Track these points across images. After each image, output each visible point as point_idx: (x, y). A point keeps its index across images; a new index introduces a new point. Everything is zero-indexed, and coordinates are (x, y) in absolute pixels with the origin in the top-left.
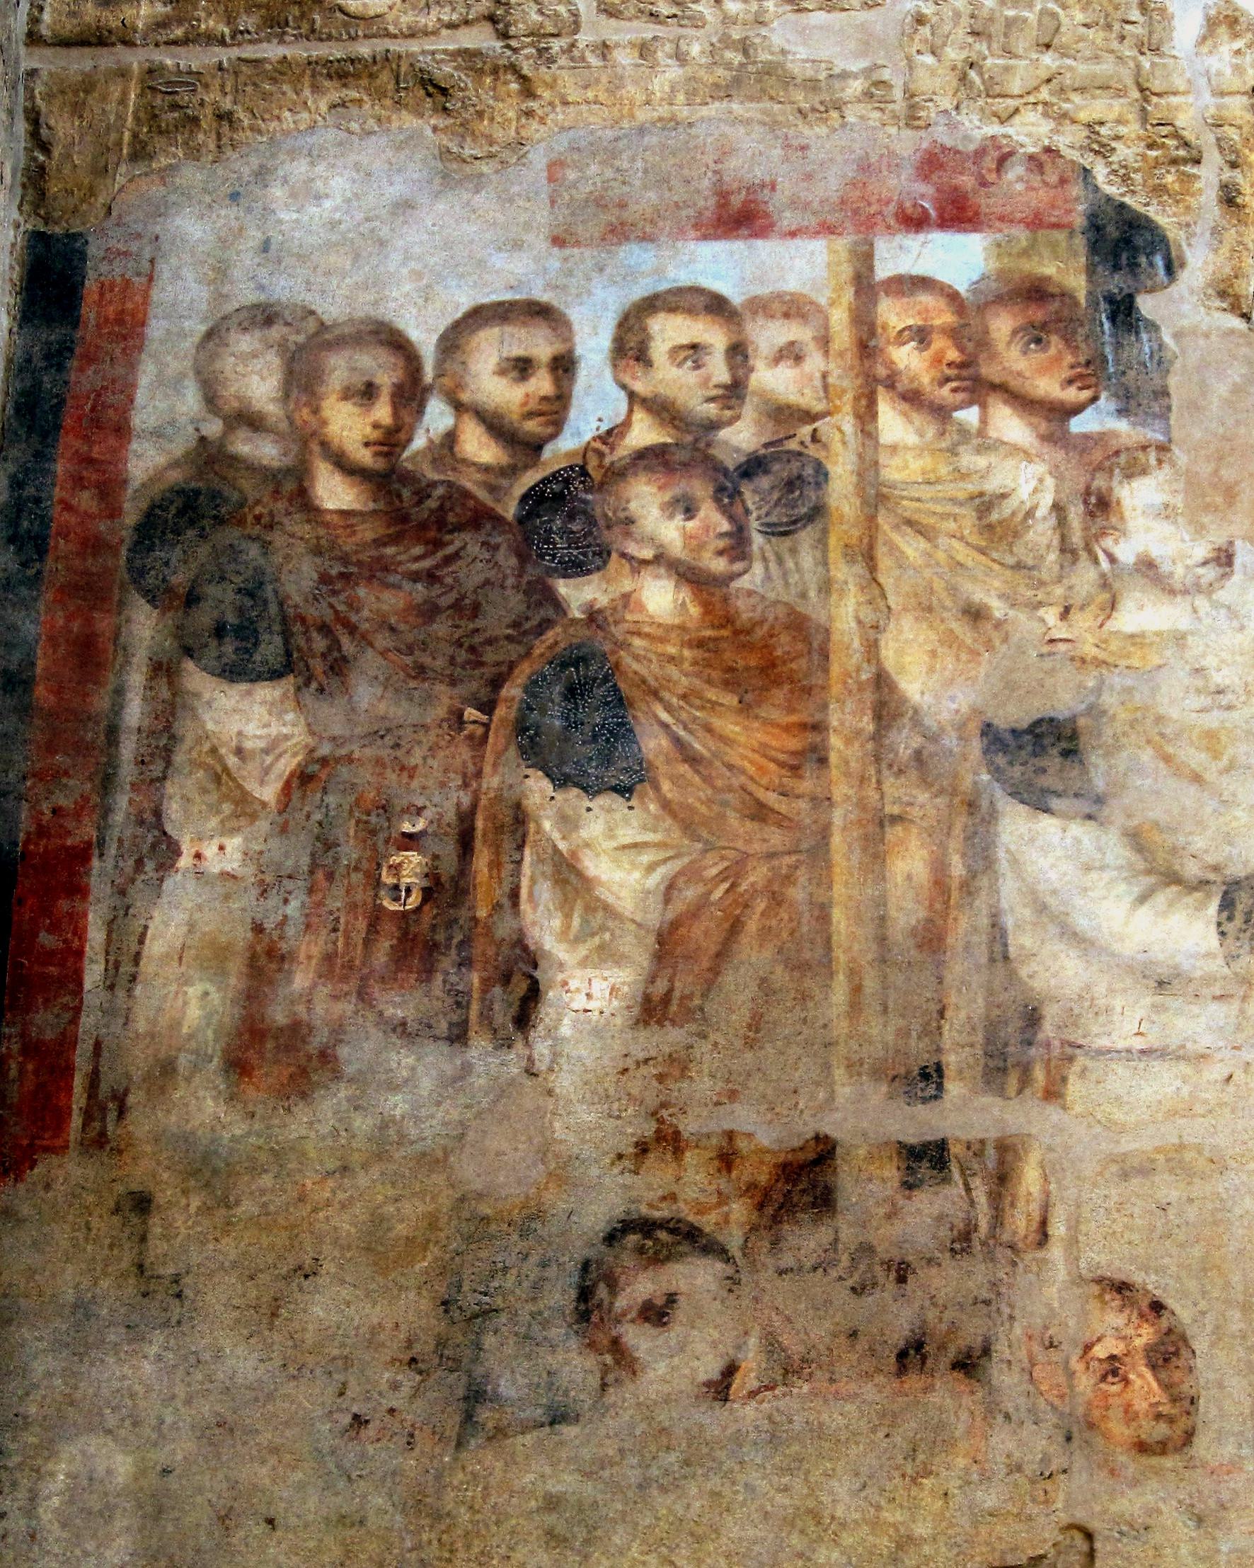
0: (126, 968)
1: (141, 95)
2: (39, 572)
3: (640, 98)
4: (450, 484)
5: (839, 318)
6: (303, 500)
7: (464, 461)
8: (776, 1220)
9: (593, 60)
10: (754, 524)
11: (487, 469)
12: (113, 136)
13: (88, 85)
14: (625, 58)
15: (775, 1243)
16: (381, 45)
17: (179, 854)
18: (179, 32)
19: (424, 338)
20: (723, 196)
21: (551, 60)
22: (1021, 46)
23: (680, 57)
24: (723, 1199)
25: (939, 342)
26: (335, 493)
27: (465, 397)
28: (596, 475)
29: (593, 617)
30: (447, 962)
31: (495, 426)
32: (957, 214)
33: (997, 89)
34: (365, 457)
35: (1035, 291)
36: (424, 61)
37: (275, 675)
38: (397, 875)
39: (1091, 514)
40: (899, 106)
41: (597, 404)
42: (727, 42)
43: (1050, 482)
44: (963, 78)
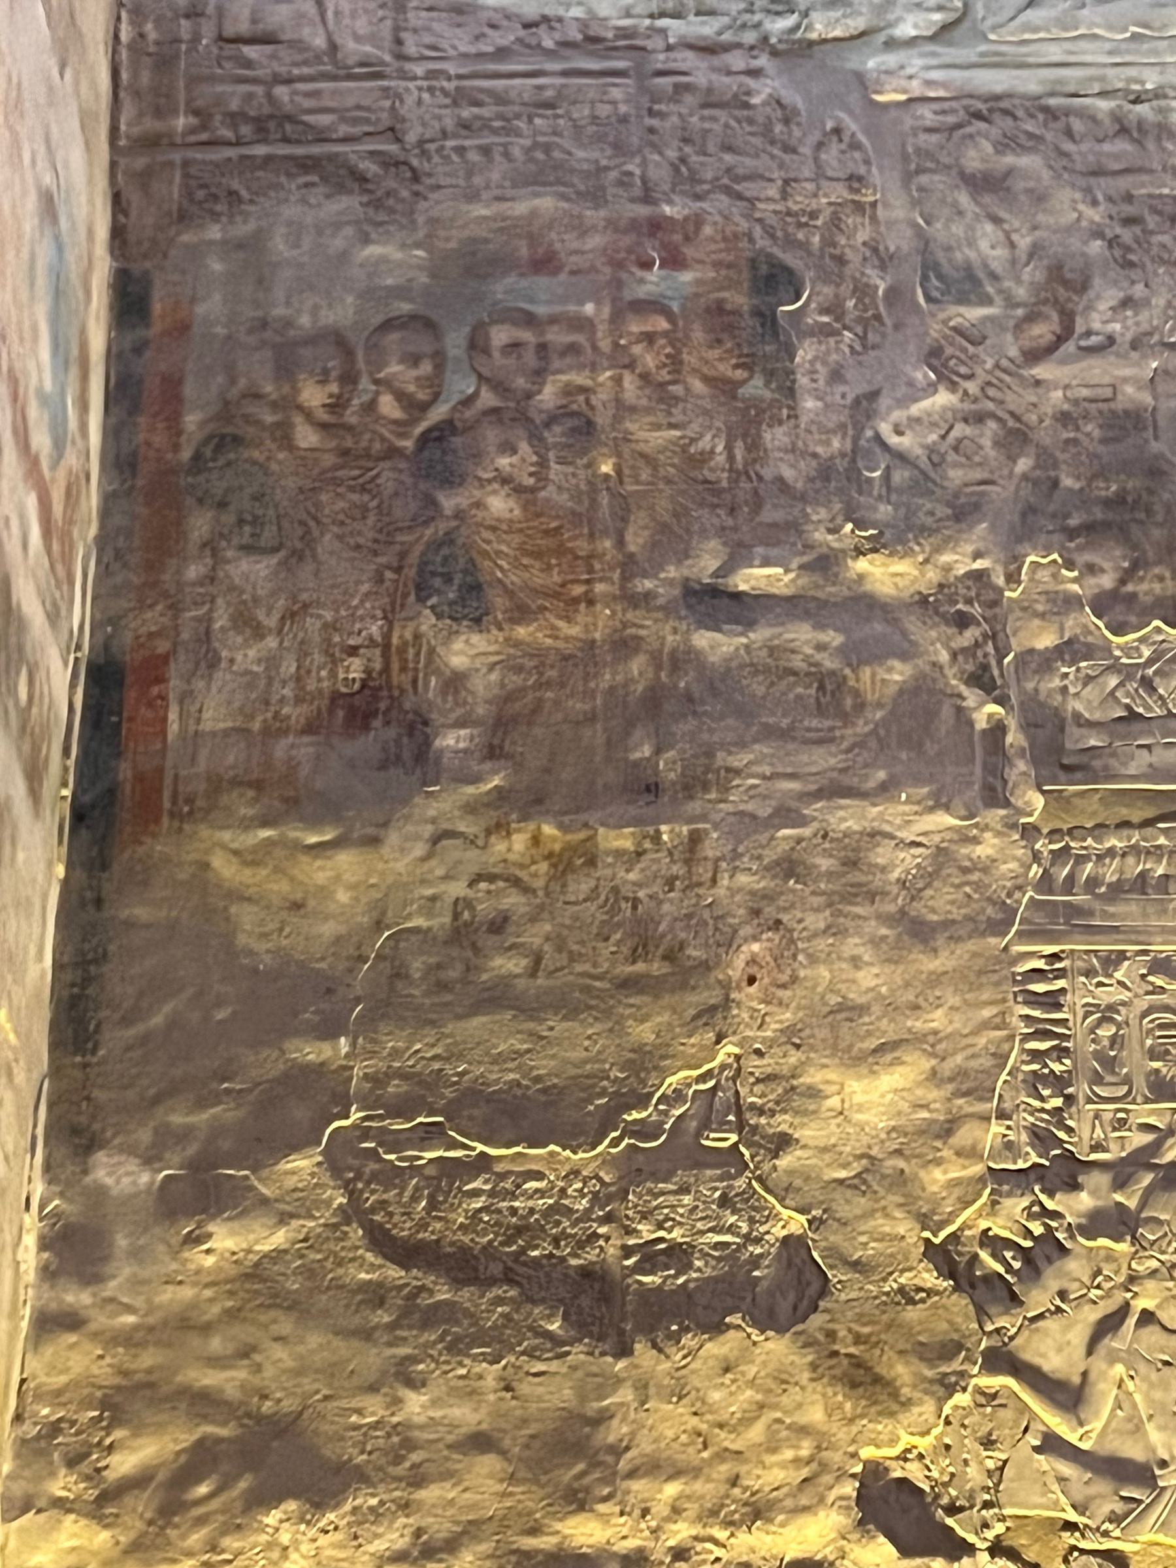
2: (132, 487)
8: (564, 872)
9: (455, 158)
10: (551, 455)
11: (396, 422)
15: (564, 886)
17: (220, 660)
18: (204, 137)
21: (429, 160)
22: (711, 148)
23: (506, 155)
24: (534, 862)
26: (306, 437)
27: (382, 375)
28: (459, 424)
29: (459, 515)
30: (377, 723)
31: (401, 397)
32: (674, 261)
34: (325, 417)
35: (719, 309)
37: (275, 550)
40: (637, 191)
42: (536, 145)
44: (677, 170)
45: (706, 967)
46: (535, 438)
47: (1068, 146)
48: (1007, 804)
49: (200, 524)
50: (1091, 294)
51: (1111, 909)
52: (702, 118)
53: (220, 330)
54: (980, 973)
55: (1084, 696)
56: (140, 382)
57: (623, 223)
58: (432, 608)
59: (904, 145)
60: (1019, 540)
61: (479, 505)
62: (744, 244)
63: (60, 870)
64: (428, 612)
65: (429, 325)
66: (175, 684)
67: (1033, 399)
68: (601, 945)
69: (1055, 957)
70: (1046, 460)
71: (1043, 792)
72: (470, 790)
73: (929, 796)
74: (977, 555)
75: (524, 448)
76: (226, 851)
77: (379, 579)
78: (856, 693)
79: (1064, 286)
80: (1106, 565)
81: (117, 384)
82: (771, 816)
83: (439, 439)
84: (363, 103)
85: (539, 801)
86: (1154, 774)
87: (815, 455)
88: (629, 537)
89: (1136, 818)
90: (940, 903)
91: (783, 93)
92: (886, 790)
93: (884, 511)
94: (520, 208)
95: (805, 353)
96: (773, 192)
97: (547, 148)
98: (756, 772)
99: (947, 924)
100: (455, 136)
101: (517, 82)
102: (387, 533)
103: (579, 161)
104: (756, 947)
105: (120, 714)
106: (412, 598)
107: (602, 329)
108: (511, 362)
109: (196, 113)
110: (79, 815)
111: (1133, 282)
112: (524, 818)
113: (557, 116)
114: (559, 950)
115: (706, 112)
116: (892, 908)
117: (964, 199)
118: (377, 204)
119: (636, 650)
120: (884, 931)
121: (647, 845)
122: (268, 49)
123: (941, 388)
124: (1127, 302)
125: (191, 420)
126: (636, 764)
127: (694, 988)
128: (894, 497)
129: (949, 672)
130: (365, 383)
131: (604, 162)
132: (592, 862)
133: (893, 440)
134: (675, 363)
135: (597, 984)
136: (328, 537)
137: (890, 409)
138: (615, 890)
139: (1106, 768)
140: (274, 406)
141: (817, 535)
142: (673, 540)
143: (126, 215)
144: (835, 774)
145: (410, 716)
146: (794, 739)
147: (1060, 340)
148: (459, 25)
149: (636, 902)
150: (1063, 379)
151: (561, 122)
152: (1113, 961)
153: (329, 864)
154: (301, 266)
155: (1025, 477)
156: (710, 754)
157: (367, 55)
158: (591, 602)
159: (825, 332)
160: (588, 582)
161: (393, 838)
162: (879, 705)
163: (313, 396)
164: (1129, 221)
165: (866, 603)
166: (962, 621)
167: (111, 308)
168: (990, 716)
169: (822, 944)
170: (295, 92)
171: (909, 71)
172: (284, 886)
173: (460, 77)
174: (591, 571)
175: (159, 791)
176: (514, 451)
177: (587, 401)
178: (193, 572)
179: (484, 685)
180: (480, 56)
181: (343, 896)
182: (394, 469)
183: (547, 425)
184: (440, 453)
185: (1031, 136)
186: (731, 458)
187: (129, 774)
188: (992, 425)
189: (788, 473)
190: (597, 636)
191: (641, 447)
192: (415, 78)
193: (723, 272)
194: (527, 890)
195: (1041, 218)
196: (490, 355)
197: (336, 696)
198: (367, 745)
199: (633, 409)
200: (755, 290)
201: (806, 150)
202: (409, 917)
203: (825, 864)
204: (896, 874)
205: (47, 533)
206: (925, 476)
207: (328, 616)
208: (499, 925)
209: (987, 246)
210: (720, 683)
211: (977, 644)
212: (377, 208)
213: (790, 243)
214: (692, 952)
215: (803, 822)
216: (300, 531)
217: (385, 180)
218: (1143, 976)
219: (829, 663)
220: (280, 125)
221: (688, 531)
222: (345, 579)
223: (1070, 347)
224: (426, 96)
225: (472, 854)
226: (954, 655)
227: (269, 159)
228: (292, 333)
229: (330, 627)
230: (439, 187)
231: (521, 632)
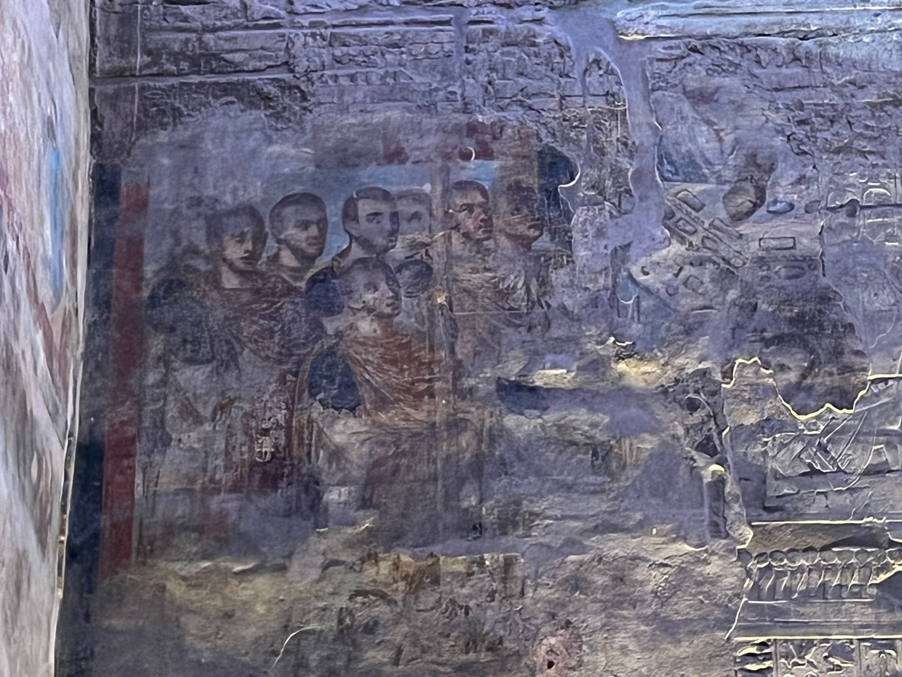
0: (152, 489)
1: (140, 99)
2: (108, 318)
3: (350, 101)
4: (277, 276)
5: (436, 202)
6: (217, 284)
7: (282, 266)
9: (330, 82)
10: (402, 292)
11: (293, 269)
12: (129, 119)
13: (116, 95)
15: (417, 598)
16: (241, 77)
17: (171, 439)
18: (155, 70)
19: (265, 212)
20: (387, 147)
21: (313, 84)
22: (510, 73)
23: (367, 81)
24: (396, 582)
25: (477, 210)
26: (230, 281)
27: (282, 237)
28: (337, 272)
29: (339, 335)
30: (283, 484)
32: (485, 153)
33: (501, 95)
34: (240, 265)
35: (517, 188)
37: (208, 361)
38: (261, 447)
39: (540, 286)
40: (459, 105)
41: (338, 242)
43: (523, 272)
45: (518, 655)
46: (391, 280)
47: (757, 71)
48: (727, 536)
49: (156, 345)
50: (777, 173)
51: (802, 610)
52: (502, 54)
53: (167, 206)
54: (711, 657)
55: (781, 459)
56: (113, 244)
57: (449, 128)
58: (320, 401)
59: (644, 71)
60: (731, 347)
61: (351, 327)
62: (534, 141)
63: (60, 593)
64: (317, 404)
66: (140, 459)
67: (738, 248)
68: (443, 640)
69: (764, 644)
70: (748, 290)
71: (752, 527)
72: (350, 530)
73: (672, 530)
74: (702, 359)
75: (383, 286)
76: (177, 575)
77: (282, 380)
78: (620, 457)
79: (757, 170)
80: (791, 365)
81: (96, 246)
82: (562, 546)
83: (322, 281)
84: (267, 46)
85: (398, 538)
86: (830, 513)
87: (586, 289)
88: (457, 349)
89: (819, 543)
90: (682, 607)
91: (559, 35)
92: (642, 527)
93: (636, 328)
94: (378, 118)
95: (579, 216)
96: (553, 104)
97: (395, 76)
98: (553, 513)
99: (687, 622)
100: (332, 67)
101: (373, 29)
102: (288, 350)
103: (419, 84)
104: (553, 641)
105: (101, 481)
106: (306, 394)
107: (436, 202)
108: (373, 225)
109: (149, 53)
110: (73, 554)
111: (805, 166)
112: (387, 551)
113: (402, 53)
114: (414, 644)
115: (506, 49)
116: (649, 611)
117: (686, 107)
118: (277, 116)
119: (465, 429)
120: (643, 628)
121: (475, 569)
123: (674, 241)
124: (801, 180)
125: (149, 270)
126: (466, 510)
127: (510, 671)
128: (642, 318)
129: (685, 442)
130: (271, 243)
131: (435, 85)
132: (436, 581)
133: (641, 278)
134: (487, 224)
135: (441, 669)
136: (246, 352)
137: (639, 256)
138: (453, 601)
139: (796, 509)
140: (207, 259)
141: (589, 346)
142: (489, 347)
143: (101, 126)
144: (606, 517)
145: (306, 478)
146: (576, 491)
147: (756, 206)
149: (467, 610)
151: (404, 56)
152: (803, 648)
153: (250, 586)
154: (224, 161)
155: (734, 303)
156: (518, 503)
158: (432, 396)
159: (591, 203)
160: (430, 381)
161: (295, 566)
162: (637, 466)
163: (235, 252)
164: (801, 123)
165: (625, 393)
166: (693, 406)
167: (92, 191)
168: (714, 472)
169: (600, 637)
170: (219, 38)
171: (646, 19)
172: (218, 602)
173: (334, 26)
174: (432, 373)
175: (130, 535)
176: (376, 289)
177: (427, 254)
178: (152, 378)
179: (359, 454)
181: (260, 609)
182: (293, 303)
183: (399, 270)
184: (325, 291)
185: (731, 63)
186: (528, 291)
187: (108, 524)
188: (710, 266)
189: (568, 303)
190: (437, 419)
191: (465, 285)
192: (302, 27)
193: (520, 161)
194: (391, 602)
195: (741, 121)
196: (358, 222)
197: (253, 465)
198: (276, 499)
199: (459, 258)
200: (542, 175)
201: (576, 74)
202: (308, 622)
203: (600, 580)
204: (649, 588)
205: (49, 359)
206: (664, 305)
207: (247, 407)
208: (371, 628)
209: (703, 141)
210: (522, 453)
211: (703, 422)
213: (566, 140)
214: (506, 644)
215: (583, 550)
216: (225, 348)
217: (280, 97)
218: (826, 657)
219: (600, 436)
220: (208, 62)
221: (499, 343)
222: (258, 382)
223: (762, 211)
224: (310, 40)
225: (351, 576)
226: (687, 431)
227: (201, 85)
228: (218, 207)
229: (250, 415)
230: (320, 104)
231: (383, 417)
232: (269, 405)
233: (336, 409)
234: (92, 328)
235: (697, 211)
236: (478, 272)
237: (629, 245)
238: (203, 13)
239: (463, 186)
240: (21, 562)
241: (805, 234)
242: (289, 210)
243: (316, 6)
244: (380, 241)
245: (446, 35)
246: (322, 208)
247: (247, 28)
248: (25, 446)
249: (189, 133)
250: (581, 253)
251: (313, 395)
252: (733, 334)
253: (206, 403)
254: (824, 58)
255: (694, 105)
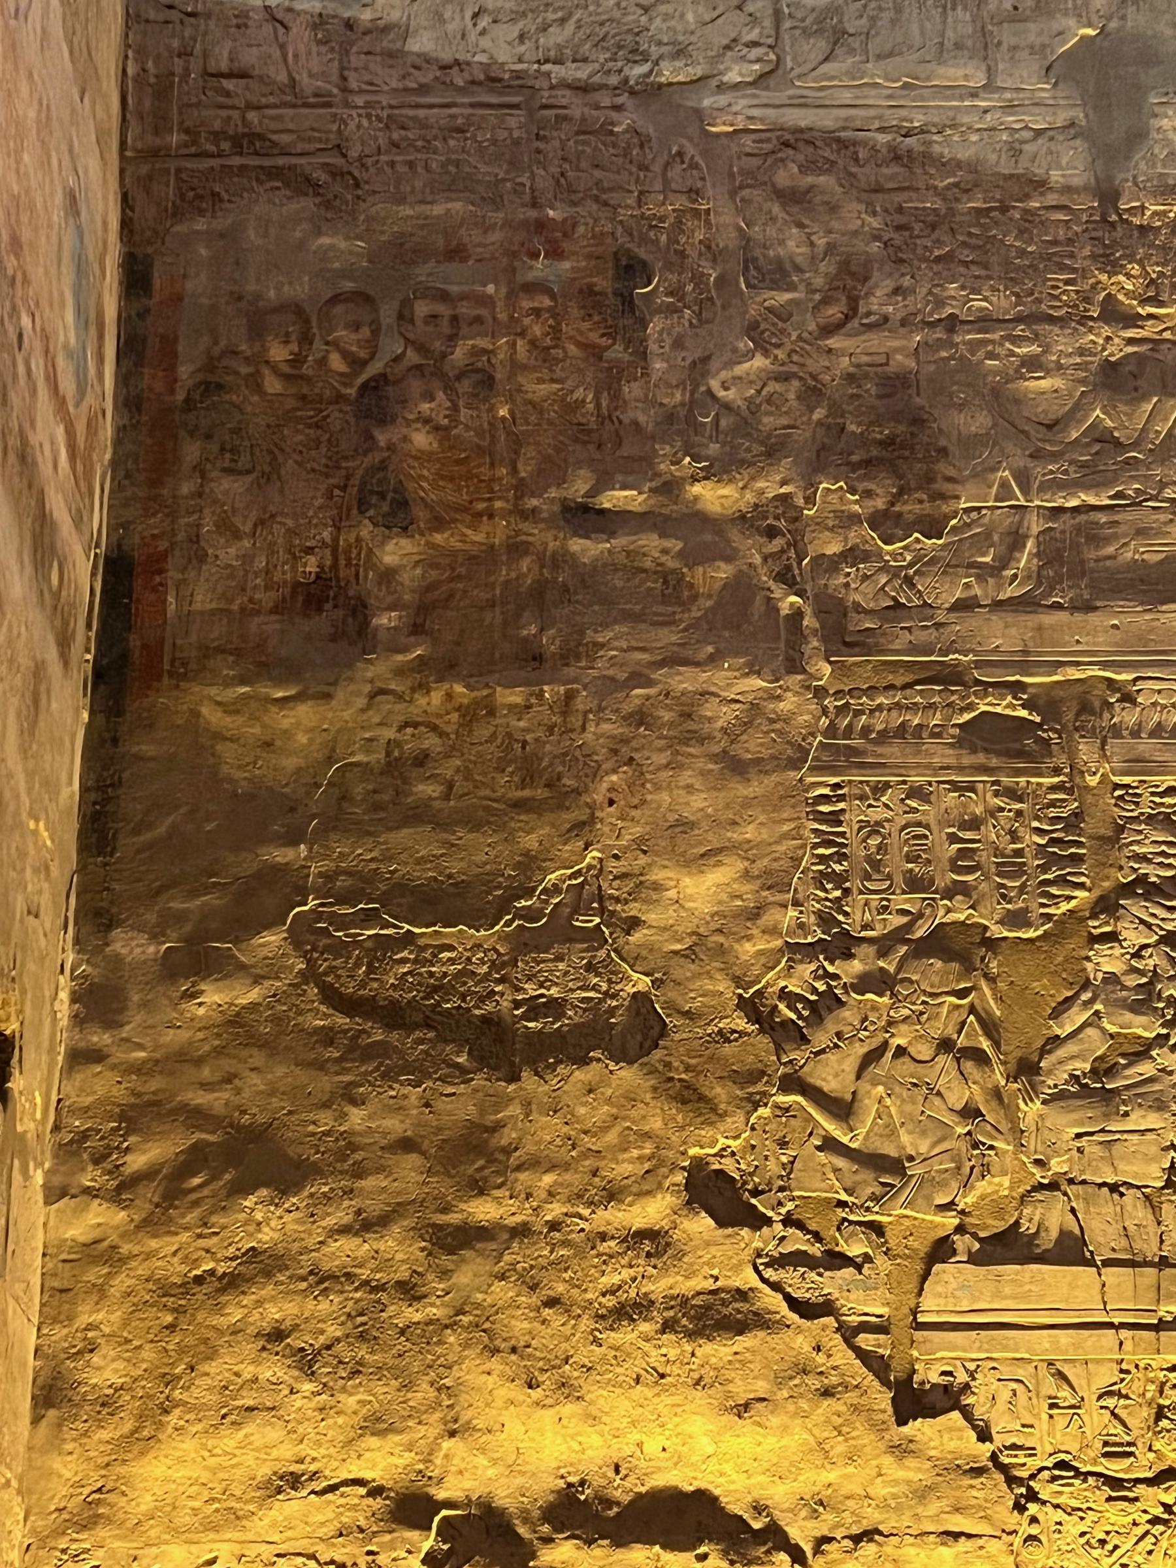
0: (186, 608)
3: (408, 189)
6: (258, 388)
9: (388, 170)
10: (461, 403)
11: (342, 374)
14: (401, 169)
15: (471, 731)
18: (193, 150)
21: (367, 170)
22: (584, 165)
23: (427, 168)
26: (273, 385)
28: (390, 377)
29: (391, 447)
30: (328, 606)
31: (346, 355)
32: (556, 253)
34: (286, 369)
35: (589, 293)
36: (308, 170)
37: (248, 472)
39: (611, 400)
40: (527, 198)
45: (578, 792)
46: (448, 388)
48: (804, 671)
49: (191, 451)
50: (871, 283)
51: (880, 750)
52: (576, 142)
53: (205, 301)
54: (781, 798)
55: (861, 590)
56: (144, 340)
58: (370, 518)
59: (731, 166)
60: (816, 471)
61: (406, 439)
62: (609, 240)
63: (85, 715)
65: (368, 299)
66: (173, 574)
67: (827, 364)
68: (498, 776)
69: (837, 786)
70: (835, 409)
71: (830, 663)
72: (400, 658)
73: (745, 664)
74: (783, 483)
75: (440, 395)
78: (691, 586)
79: (850, 279)
80: (879, 491)
82: (627, 679)
84: (316, 125)
85: (452, 666)
86: (913, 649)
87: (661, 404)
88: (520, 466)
89: (899, 681)
90: (751, 745)
91: (640, 123)
92: (713, 660)
93: (714, 448)
94: (438, 210)
95: (654, 327)
97: (457, 164)
98: (617, 647)
99: (758, 761)
100: (388, 152)
101: (435, 111)
103: (484, 174)
104: (614, 778)
105: (130, 598)
106: (355, 511)
107: (500, 305)
108: (430, 328)
109: (187, 131)
110: (99, 674)
111: (903, 275)
112: (440, 680)
114: (466, 779)
116: (716, 749)
117: (776, 209)
118: (328, 205)
119: (526, 553)
120: (711, 766)
121: (533, 701)
122: (243, 82)
123: (758, 355)
124: (897, 291)
125: (185, 370)
126: (525, 640)
127: (568, 809)
128: (721, 437)
129: (763, 571)
130: (318, 344)
132: (492, 713)
133: (721, 394)
134: (556, 331)
135: (495, 805)
136: (291, 461)
137: (719, 370)
138: (509, 735)
139: (877, 644)
141: (662, 466)
142: (554, 469)
144: (675, 649)
146: (644, 621)
147: (847, 318)
148: (391, 67)
149: (524, 743)
150: (850, 350)
152: (879, 789)
153: (292, 713)
155: (820, 423)
156: (582, 633)
157: (319, 88)
158: (491, 516)
159: (671, 310)
160: (490, 499)
161: (340, 694)
162: (710, 596)
164: (899, 228)
165: (701, 519)
166: (772, 533)
167: (121, 283)
168: (792, 604)
169: (665, 774)
171: (735, 109)
172: (257, 730)
173: (391, 107)
174: (491, 491)
175: (162, 657)
176: (433, 399)
177: (489, 360)
178: (186, 488)
179: (410, 578)
180: (406, 90)
181: (302, 739)
182: (341, 411)
183: (458, 379)
184: (376, 400)
186: (598, 406)
187: (138, 643)
188: (796, 383)
189: (642, 419)
190: (497, 541)
191: (530, 396)
192: (356, 107)
193: (593, 262)
194: (442, 734)
195: (835, 224)
198: (322, 623)
199: (524, 367)
200: (617, 278)
201: (657, 168)
202: (352, 754)
203: (667, 716)
204: (720, 723)
205: (72, 457)
206: (745, 421)
207: (290, 523)
208: (421, 759)
209: (794, 246)
210: (589, 578)
211: (782, 551)
212: (327, 209)
213: (644, 240)
214: (565, 781)
215: (650, 683)
216: (268, 459)
217: (334, 187)
218: (902, 800)
219: (671, 564)
220: (252, 143)
221: (565, 460)
223: (855, 323)
224: (365, 122)
225: (399, 707)
226: (765, 559)
227: (243, 168)
228: (261, 304)
230: (374, 192)
231: (438, 538)
232: (315, 521)
233: (388, 528)
234: (121, 433)
235: (785, 321)
236: (544, 382)
237: (709, 357)
238: (247, 88)
239: (532, 288)
240: (38, 670)
241: (899, 349)
242: (339, 309)
243: (371, 84)
244: (438, 345)
245: (515, 120)
246: (376, 310)
247: (294, 106)
248: (42, 545)
249: (229, 221)
250: (658, 365)
251: (361, 512)
252: (818, 456)
253: (246, 517)
254: (928, 158)
255: (784, 205)
